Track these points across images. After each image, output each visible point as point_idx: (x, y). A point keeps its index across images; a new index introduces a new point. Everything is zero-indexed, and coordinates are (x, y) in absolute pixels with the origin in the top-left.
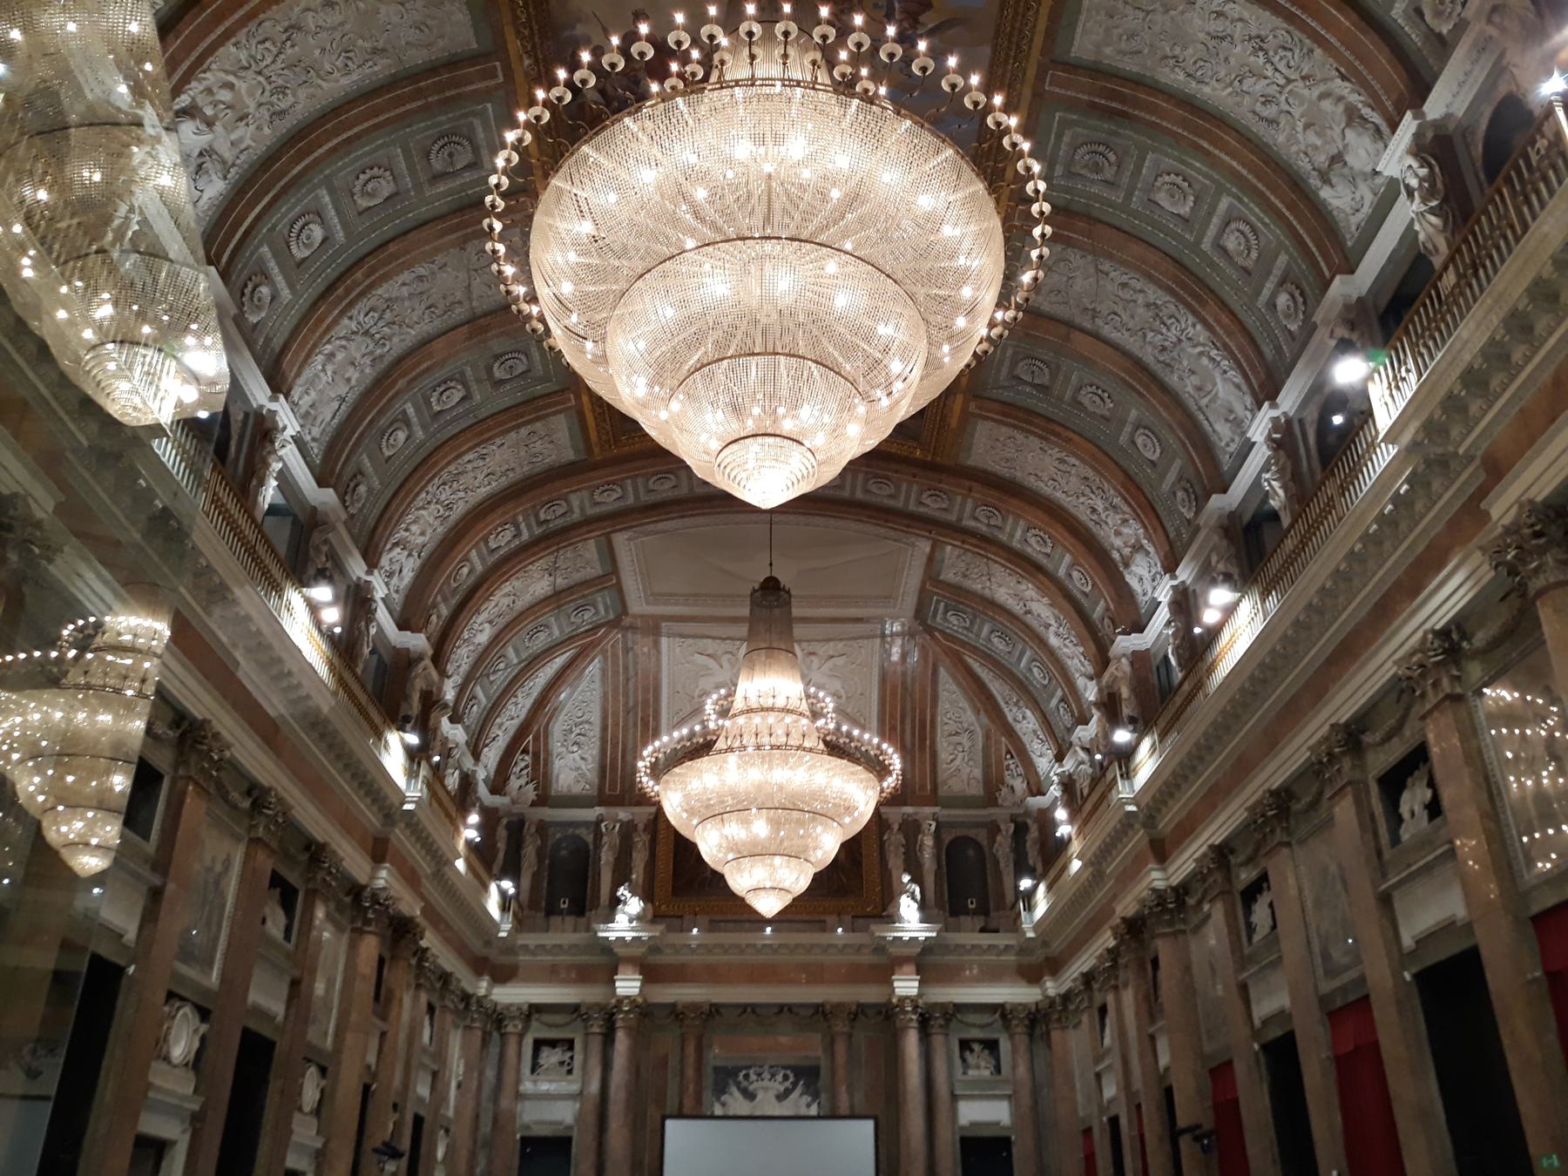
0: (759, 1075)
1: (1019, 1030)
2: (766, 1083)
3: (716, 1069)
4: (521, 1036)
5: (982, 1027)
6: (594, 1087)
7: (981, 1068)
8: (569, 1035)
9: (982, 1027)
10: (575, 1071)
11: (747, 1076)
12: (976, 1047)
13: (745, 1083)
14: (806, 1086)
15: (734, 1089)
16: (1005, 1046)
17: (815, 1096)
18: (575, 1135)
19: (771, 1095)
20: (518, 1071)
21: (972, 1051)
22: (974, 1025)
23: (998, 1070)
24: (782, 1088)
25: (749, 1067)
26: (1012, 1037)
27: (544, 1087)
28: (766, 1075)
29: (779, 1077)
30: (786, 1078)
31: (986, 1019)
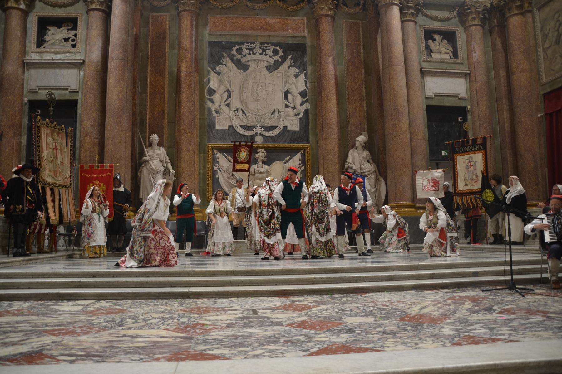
0: (251, 50)
1: (476, 22)
2: (258, 56)
3: (211, 44)
4: (25, 14)
5: (442, 20)
6: (96, 55)
7: (441, 51)
8: (74, 15)
9: (442, 20)
10: (78, 45)
11: (239, 51)
12: (437, 37)
13: (239, 56)
14: (295, 60)
15: (228, 61)
16: (461, 37)
17: (303, 67)
18: (80, 97)
19: (262, 65)
20: (24, 44)
21: (434, 40)
22: (436, 19)
23: (455, 54)
24: (272, 61)
25: (243, 43)
26: (466, 29)
27: (48, 57)
28: (258, 50)
29: (270, 52)
30: (275, 52)
31: (445, 14)
